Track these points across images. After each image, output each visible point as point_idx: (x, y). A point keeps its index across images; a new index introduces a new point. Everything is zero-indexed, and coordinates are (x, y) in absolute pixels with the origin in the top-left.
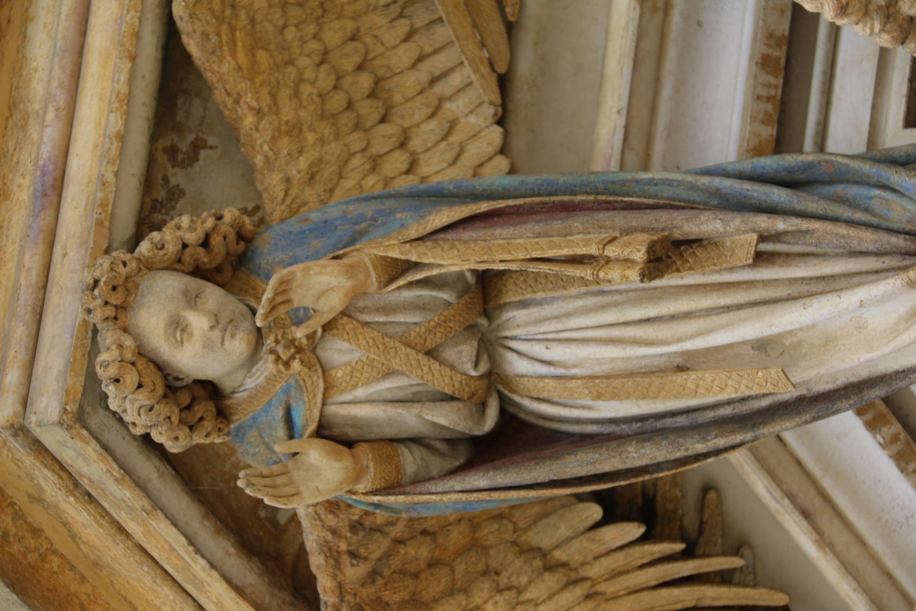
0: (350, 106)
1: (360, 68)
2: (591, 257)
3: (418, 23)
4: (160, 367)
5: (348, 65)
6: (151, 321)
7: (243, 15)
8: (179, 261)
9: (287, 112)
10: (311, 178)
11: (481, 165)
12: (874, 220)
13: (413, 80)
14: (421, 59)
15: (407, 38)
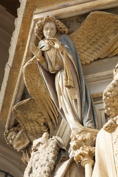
0: (90, 40)
1: (97, 39)
2: (68, 78)
3: (105, 44)
4: (43, 29)
5: (96, 37)
6: (47, 25)
7: (94, 22)
8: (57, 26)
9: (86, 32)
10: (78, 38)
11: (88, 59)
12: (83, 113)
13: (97, 46)
14: (101, 46)
15: (103, 44)
